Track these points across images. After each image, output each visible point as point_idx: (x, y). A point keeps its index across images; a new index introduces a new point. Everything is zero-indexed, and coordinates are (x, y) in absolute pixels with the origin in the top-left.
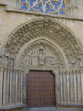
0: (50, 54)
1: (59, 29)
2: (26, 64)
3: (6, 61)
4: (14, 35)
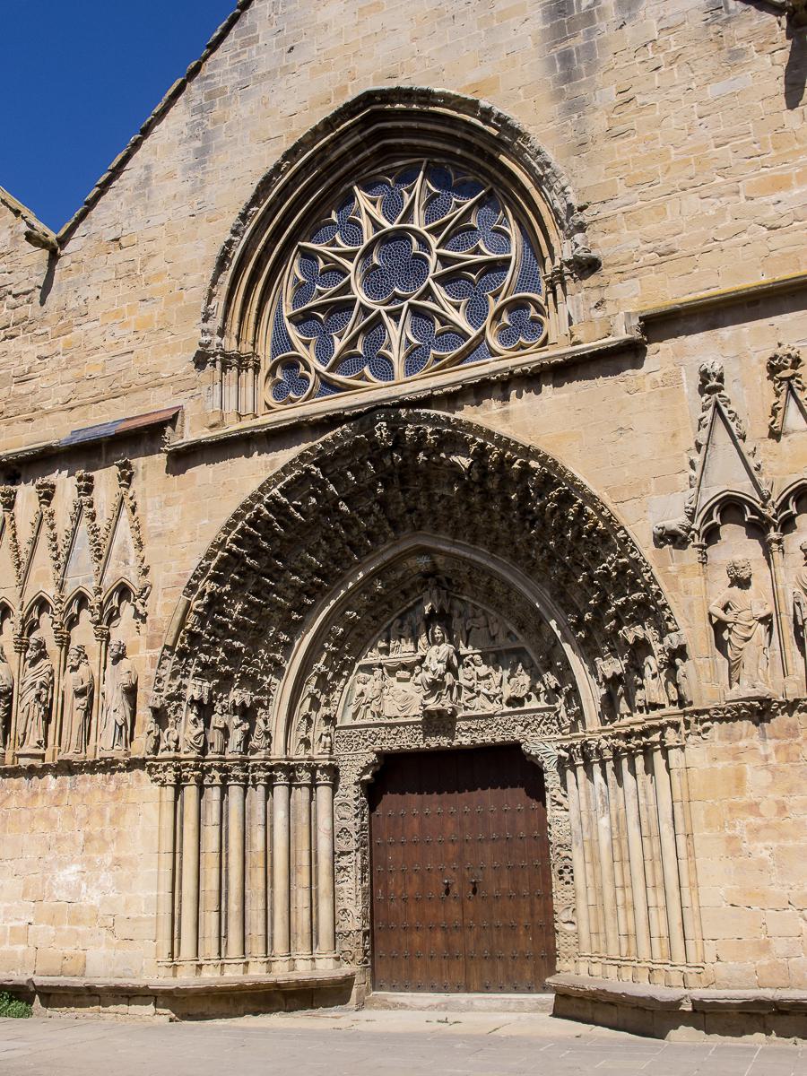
0: (495, 629)
1: (467, 466)
2: (358, 722)
3: (191, 727)
4: (214, 578)
